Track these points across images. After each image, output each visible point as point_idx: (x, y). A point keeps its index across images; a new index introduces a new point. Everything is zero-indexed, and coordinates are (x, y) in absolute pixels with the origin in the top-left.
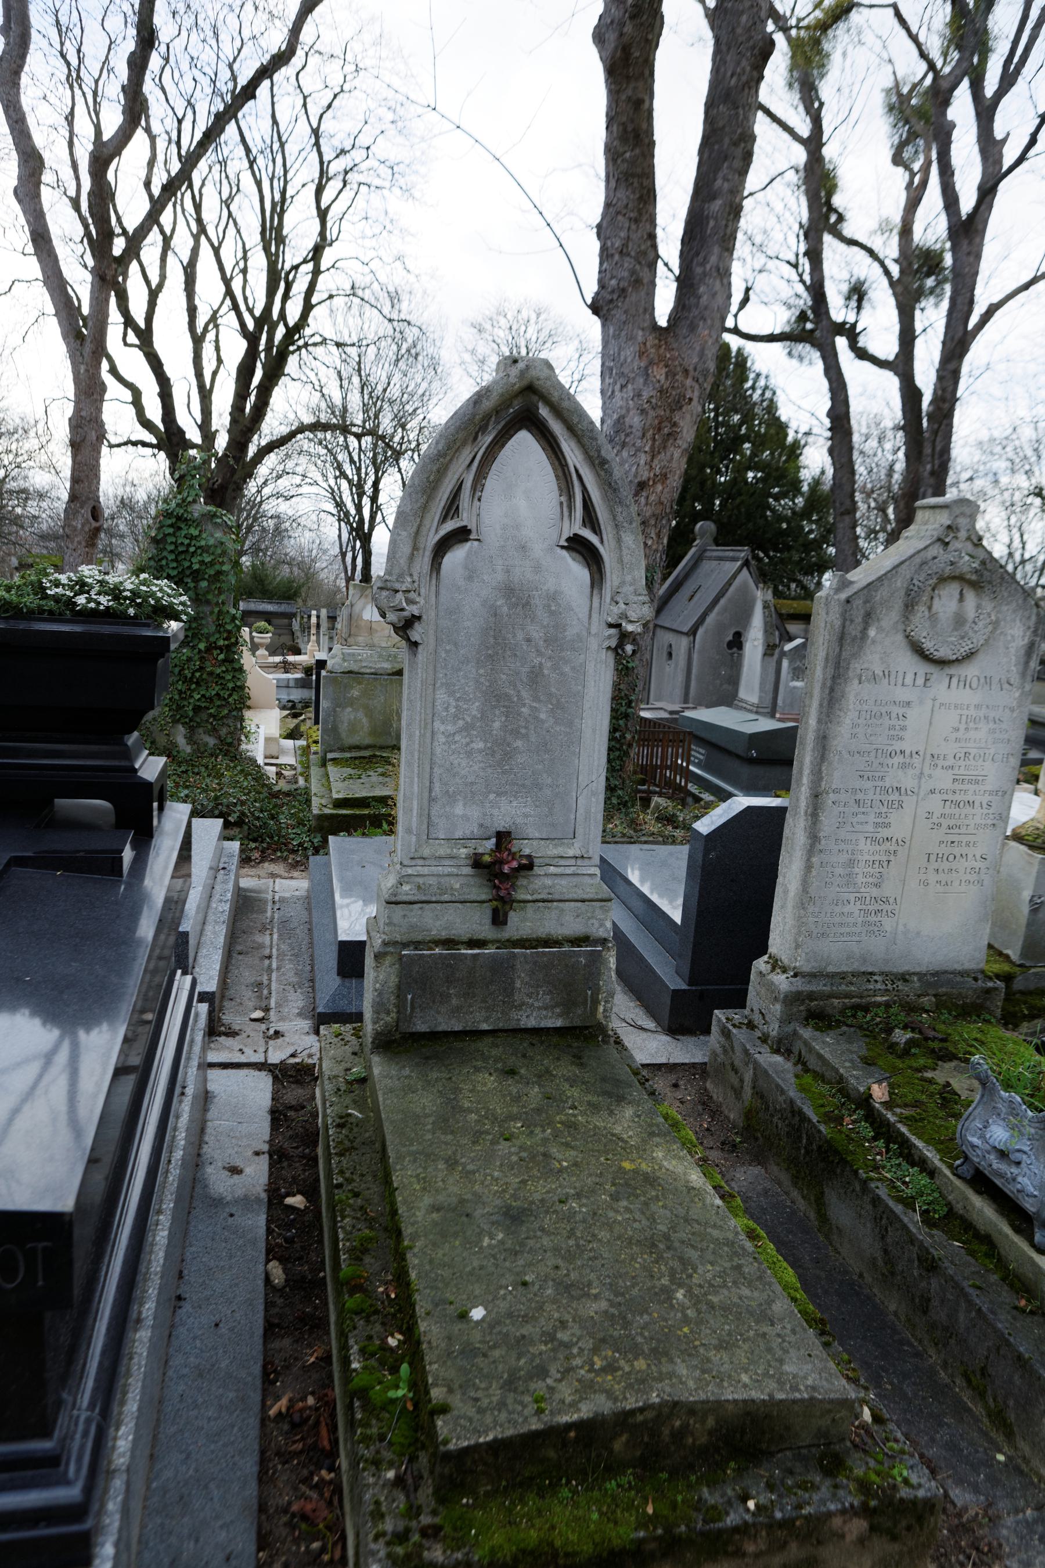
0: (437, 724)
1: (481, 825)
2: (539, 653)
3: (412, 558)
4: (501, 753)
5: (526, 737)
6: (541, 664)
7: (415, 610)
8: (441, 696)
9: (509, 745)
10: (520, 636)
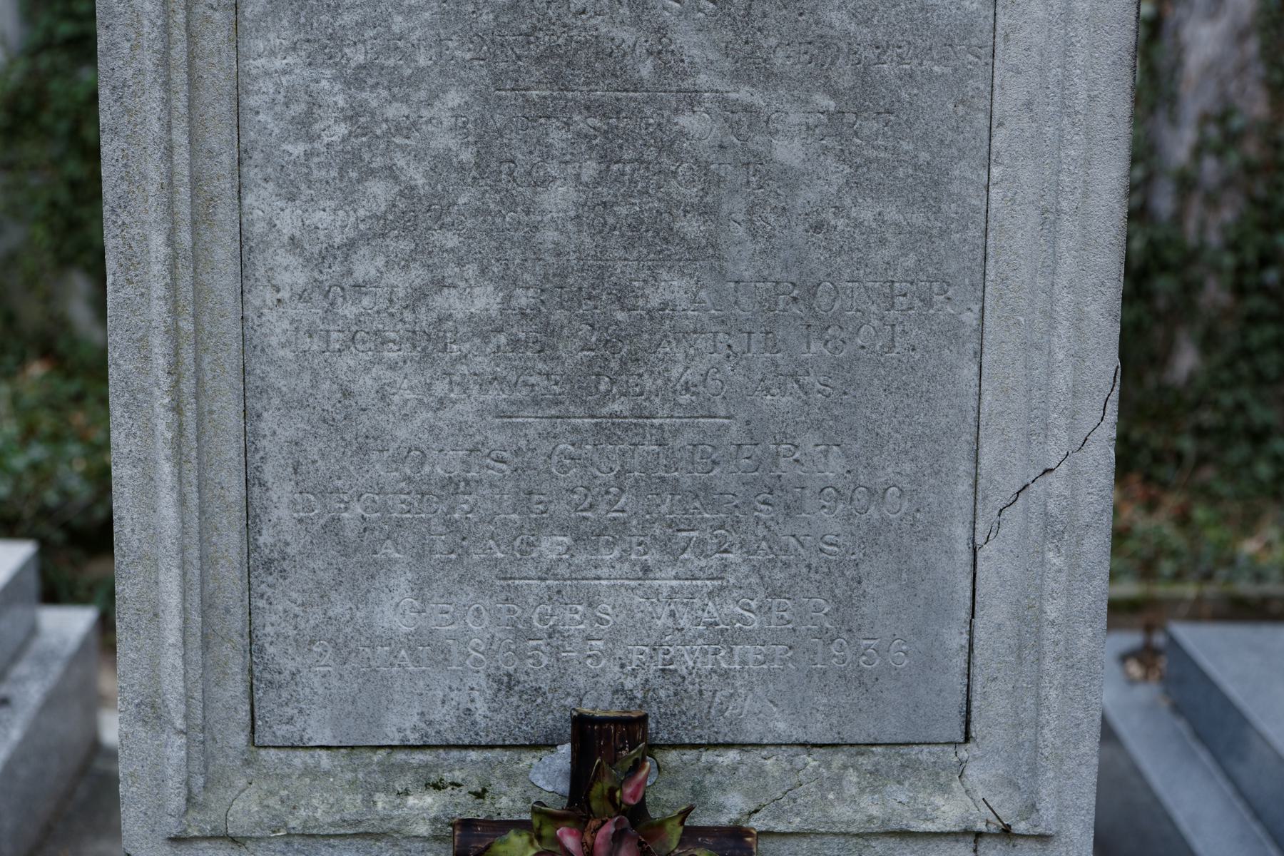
0: (262, 202)
1: (507, 684)
4: (585, 337)
5: (707, 254)
8: (274, 59)
9: (622, 296)
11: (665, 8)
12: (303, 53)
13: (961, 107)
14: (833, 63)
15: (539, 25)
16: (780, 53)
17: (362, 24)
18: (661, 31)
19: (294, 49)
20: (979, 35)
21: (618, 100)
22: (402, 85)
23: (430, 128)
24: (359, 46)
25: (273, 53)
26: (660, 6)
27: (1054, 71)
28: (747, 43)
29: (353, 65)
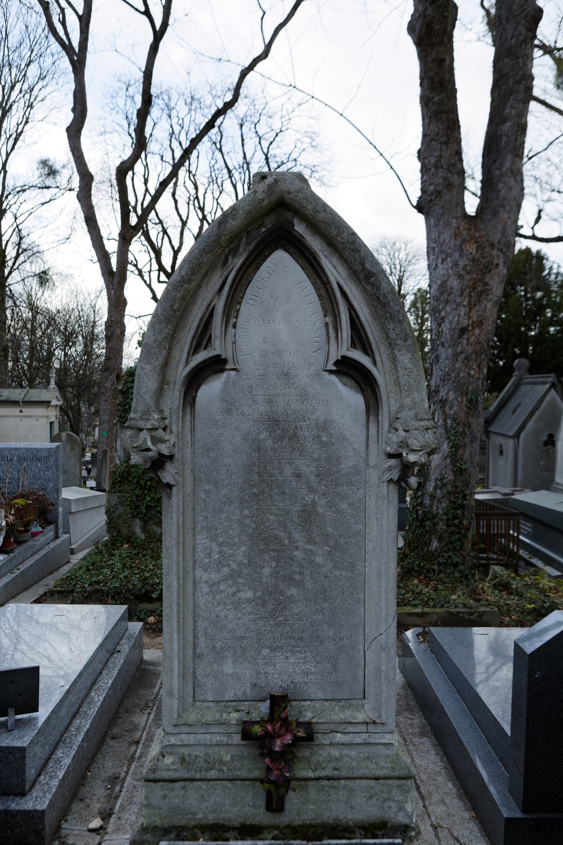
0: (199, 572)
1: (254, 685)
2: (311, 489)
3: (160, 392)
4: (273, 603)
5: (301, 584)
6: (313, 501)
7: (165, 449)
8: (202, 541)
9: (281, 593)
10: (288, 471)
17: (222, 532)
18: (290, 533)
25: (202, 539)
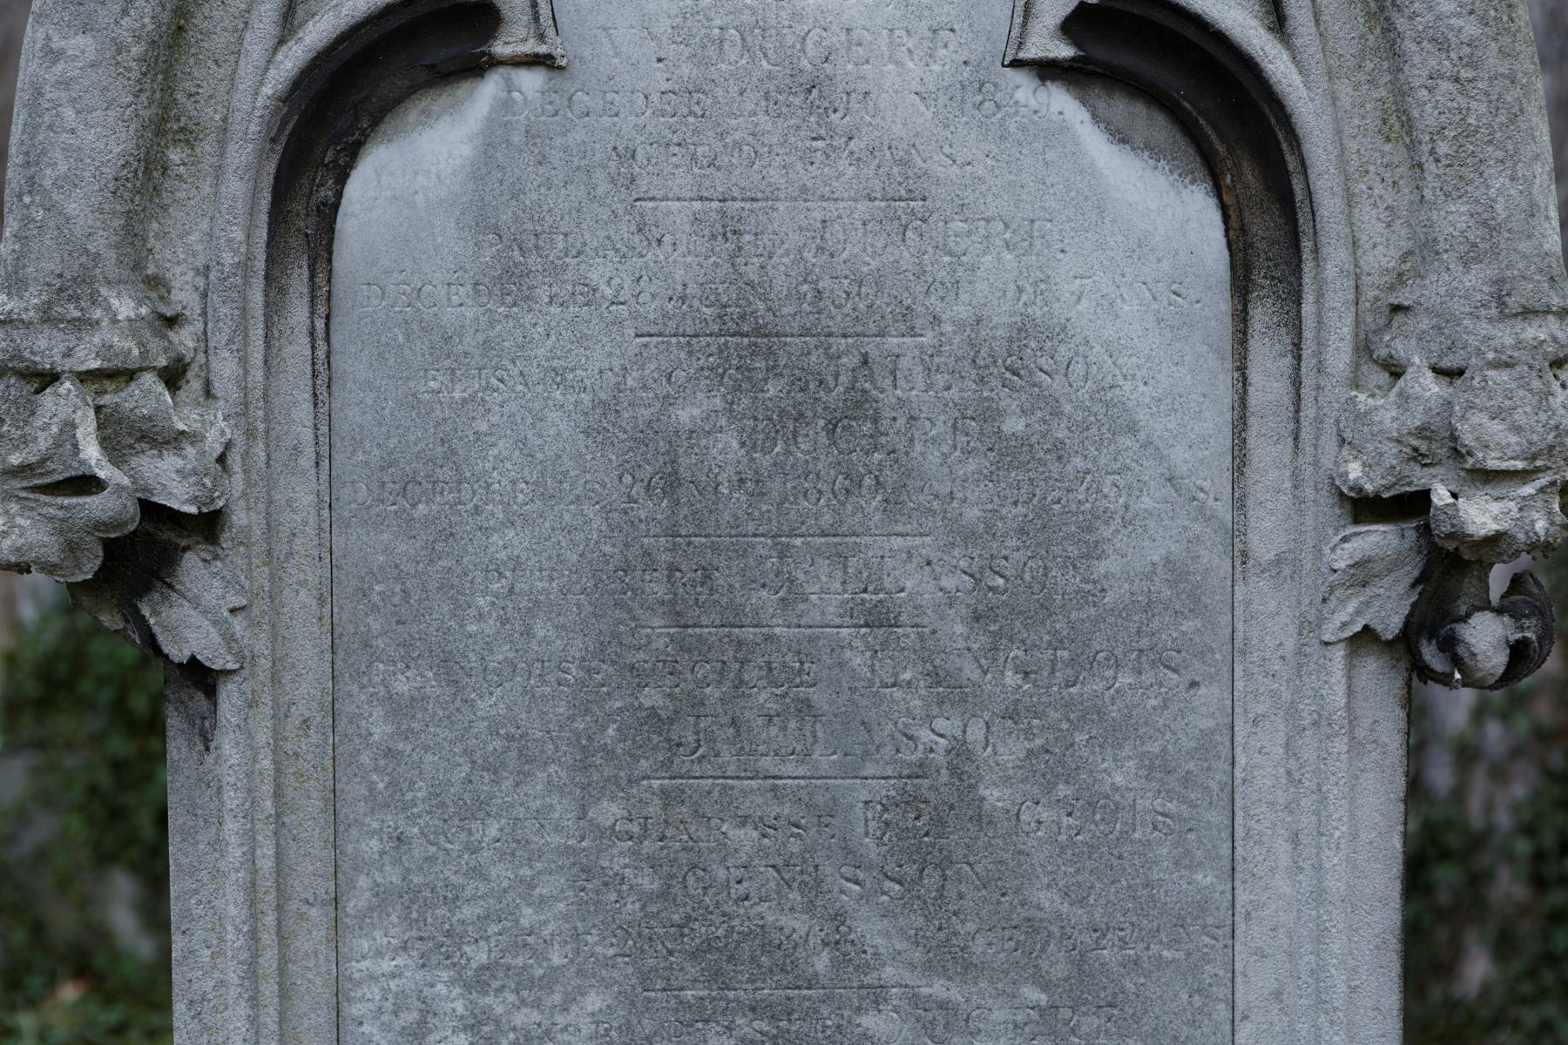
2: (947, 689)
3: (146, 180)
6: (960, 750)
7: (173, 482)
8: (381, 962)
10: (827, 596)
11: (842, 892)
12: (415, 953)
13: (1197, 997)
14: (1043, 950)
15: (694, 915)
16: (980, 940)
17: (485, 918)
18: (839, 918)
19: (405, 949)
20: (1215, 913)
21: (788, 999)
22: (531, 987)
23: (566, 1037)
24: (482, 943)
25: (379, 954)
26: (836, 889)
27: (1306, 959)
28: (940, 929)
29: (474, 965)
